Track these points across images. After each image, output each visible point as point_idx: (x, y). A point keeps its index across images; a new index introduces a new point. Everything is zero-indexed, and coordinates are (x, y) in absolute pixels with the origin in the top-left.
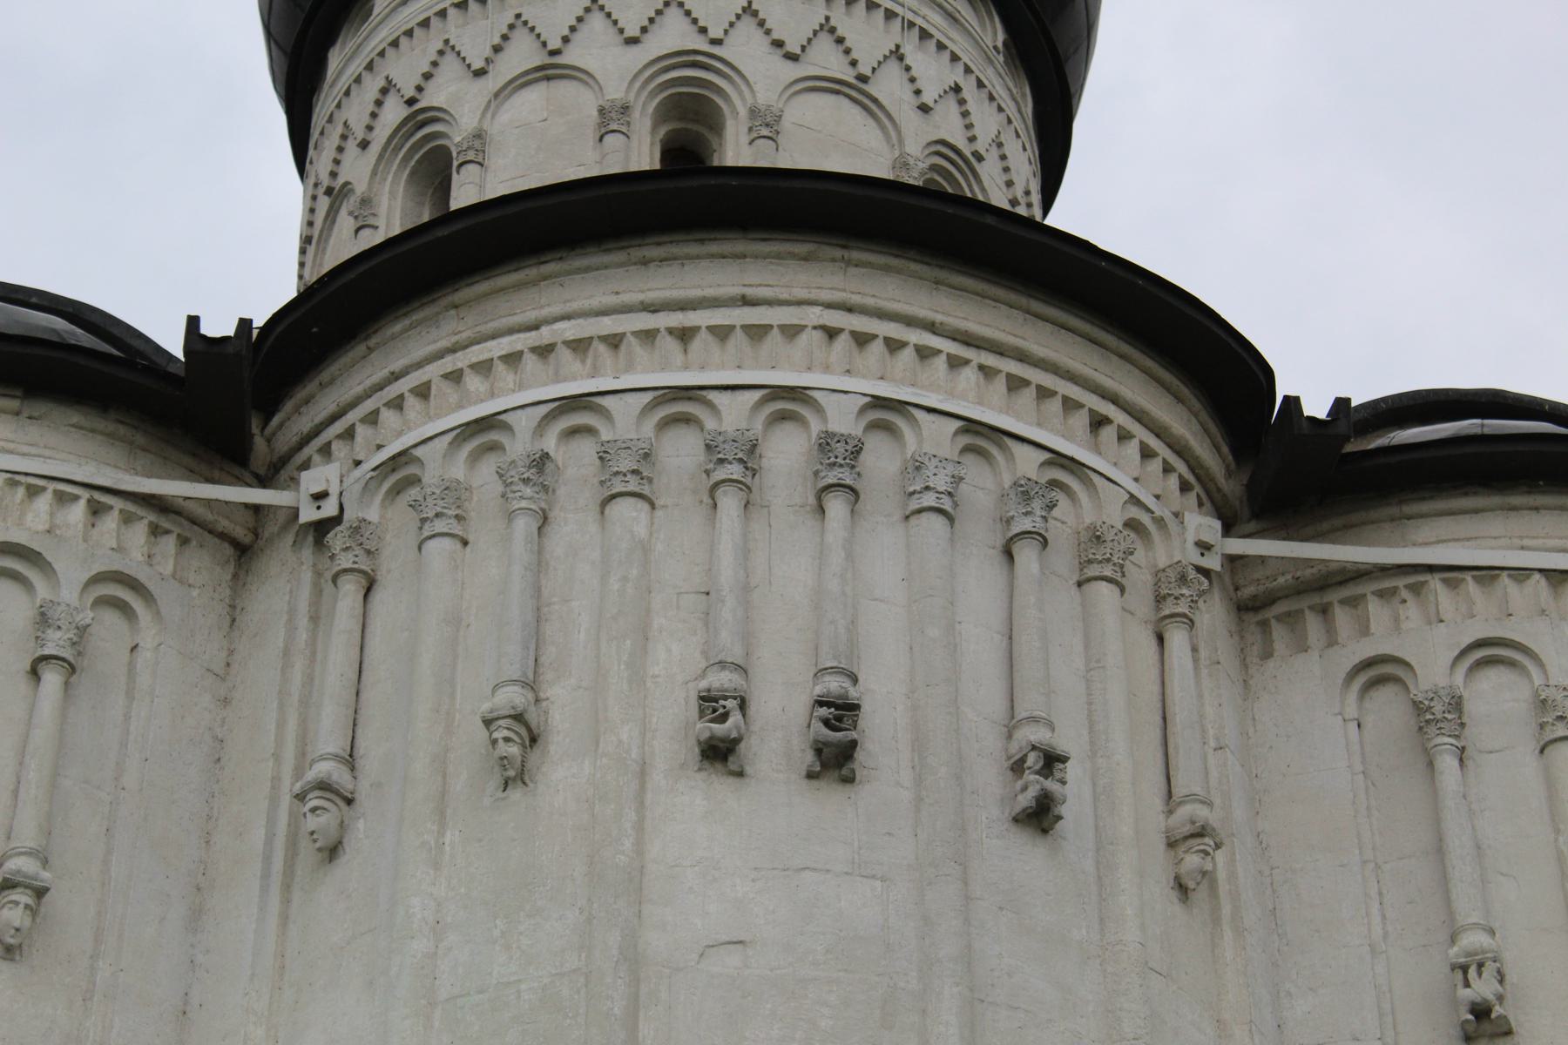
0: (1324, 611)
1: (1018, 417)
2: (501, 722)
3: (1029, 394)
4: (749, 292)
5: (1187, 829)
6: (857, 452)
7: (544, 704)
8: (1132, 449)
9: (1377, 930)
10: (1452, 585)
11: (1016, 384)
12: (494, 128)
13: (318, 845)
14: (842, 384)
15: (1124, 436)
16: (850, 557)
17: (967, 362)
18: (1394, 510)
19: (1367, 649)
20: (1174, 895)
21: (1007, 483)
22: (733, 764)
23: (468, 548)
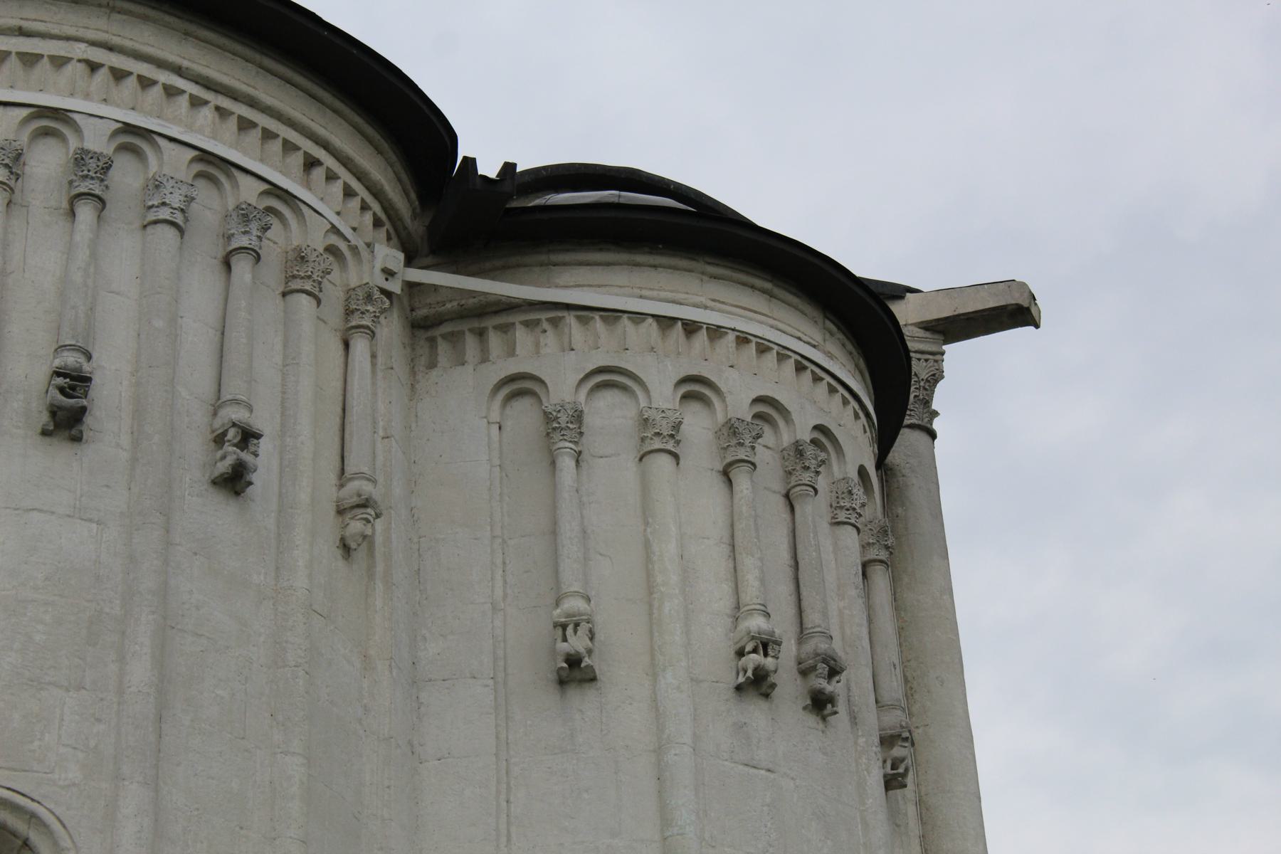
0: (481, 334)
1: (245, 153)
3: (256, 134)
4: (25, 24)
5: (355, 500)
6: (107, 168)
8: (337, 188)
9: (499, 592)
10: (584, 321)
11: (245, 125)
14: (100, 111)
15: (331, 177)
16: (94, 255)
17: (206, 103)
18: (543, 258)
19: (513, 367)
20: (339, 553)
21: (231, 207)
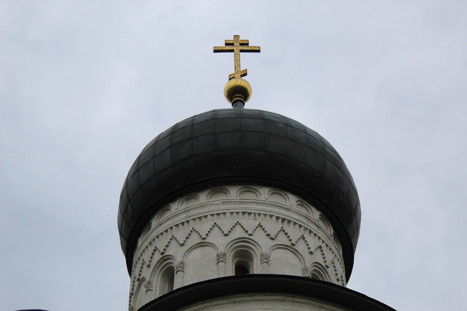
12: (187, 261)
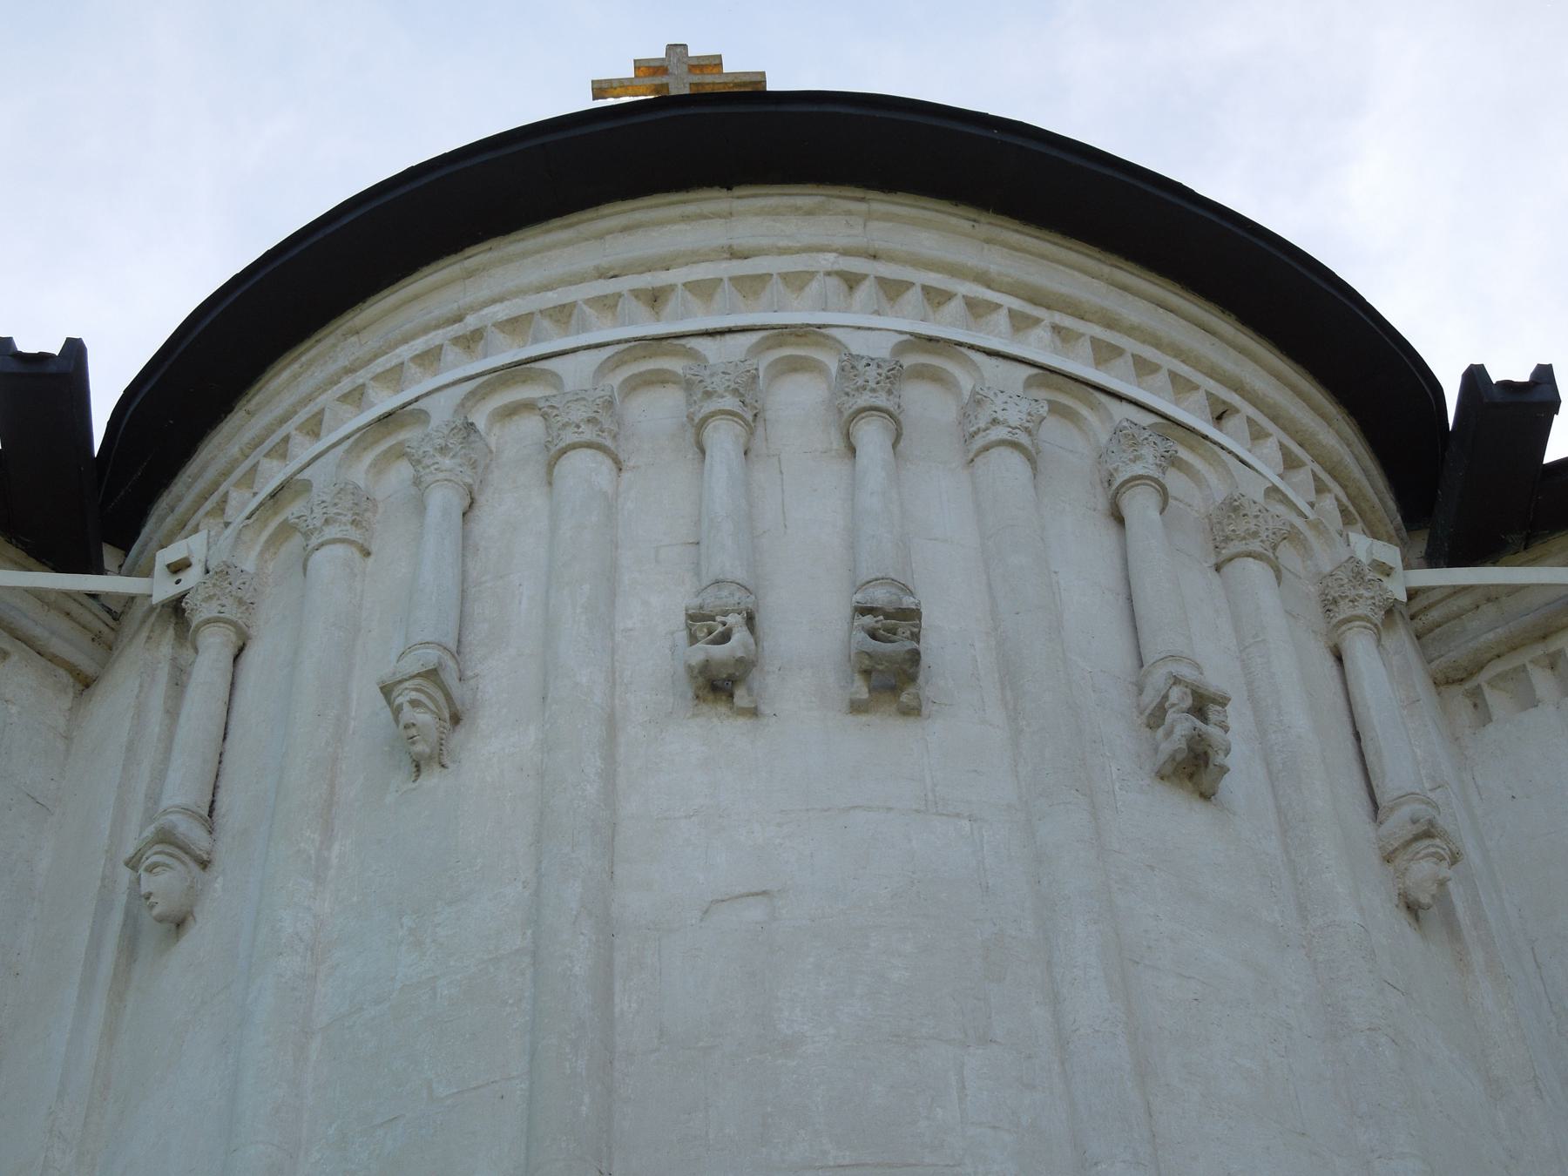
2: (407, 684)
5: (1409, 831)
7: (472, 682)
13: (156, 911)
20: (1403, 916)
21: (1104, 438)
22: (741, 697)
23: (371, 560)
